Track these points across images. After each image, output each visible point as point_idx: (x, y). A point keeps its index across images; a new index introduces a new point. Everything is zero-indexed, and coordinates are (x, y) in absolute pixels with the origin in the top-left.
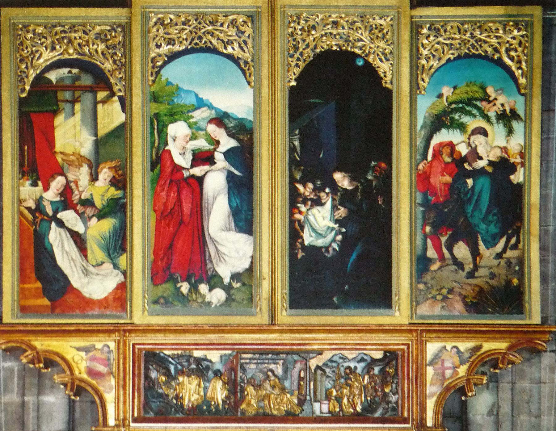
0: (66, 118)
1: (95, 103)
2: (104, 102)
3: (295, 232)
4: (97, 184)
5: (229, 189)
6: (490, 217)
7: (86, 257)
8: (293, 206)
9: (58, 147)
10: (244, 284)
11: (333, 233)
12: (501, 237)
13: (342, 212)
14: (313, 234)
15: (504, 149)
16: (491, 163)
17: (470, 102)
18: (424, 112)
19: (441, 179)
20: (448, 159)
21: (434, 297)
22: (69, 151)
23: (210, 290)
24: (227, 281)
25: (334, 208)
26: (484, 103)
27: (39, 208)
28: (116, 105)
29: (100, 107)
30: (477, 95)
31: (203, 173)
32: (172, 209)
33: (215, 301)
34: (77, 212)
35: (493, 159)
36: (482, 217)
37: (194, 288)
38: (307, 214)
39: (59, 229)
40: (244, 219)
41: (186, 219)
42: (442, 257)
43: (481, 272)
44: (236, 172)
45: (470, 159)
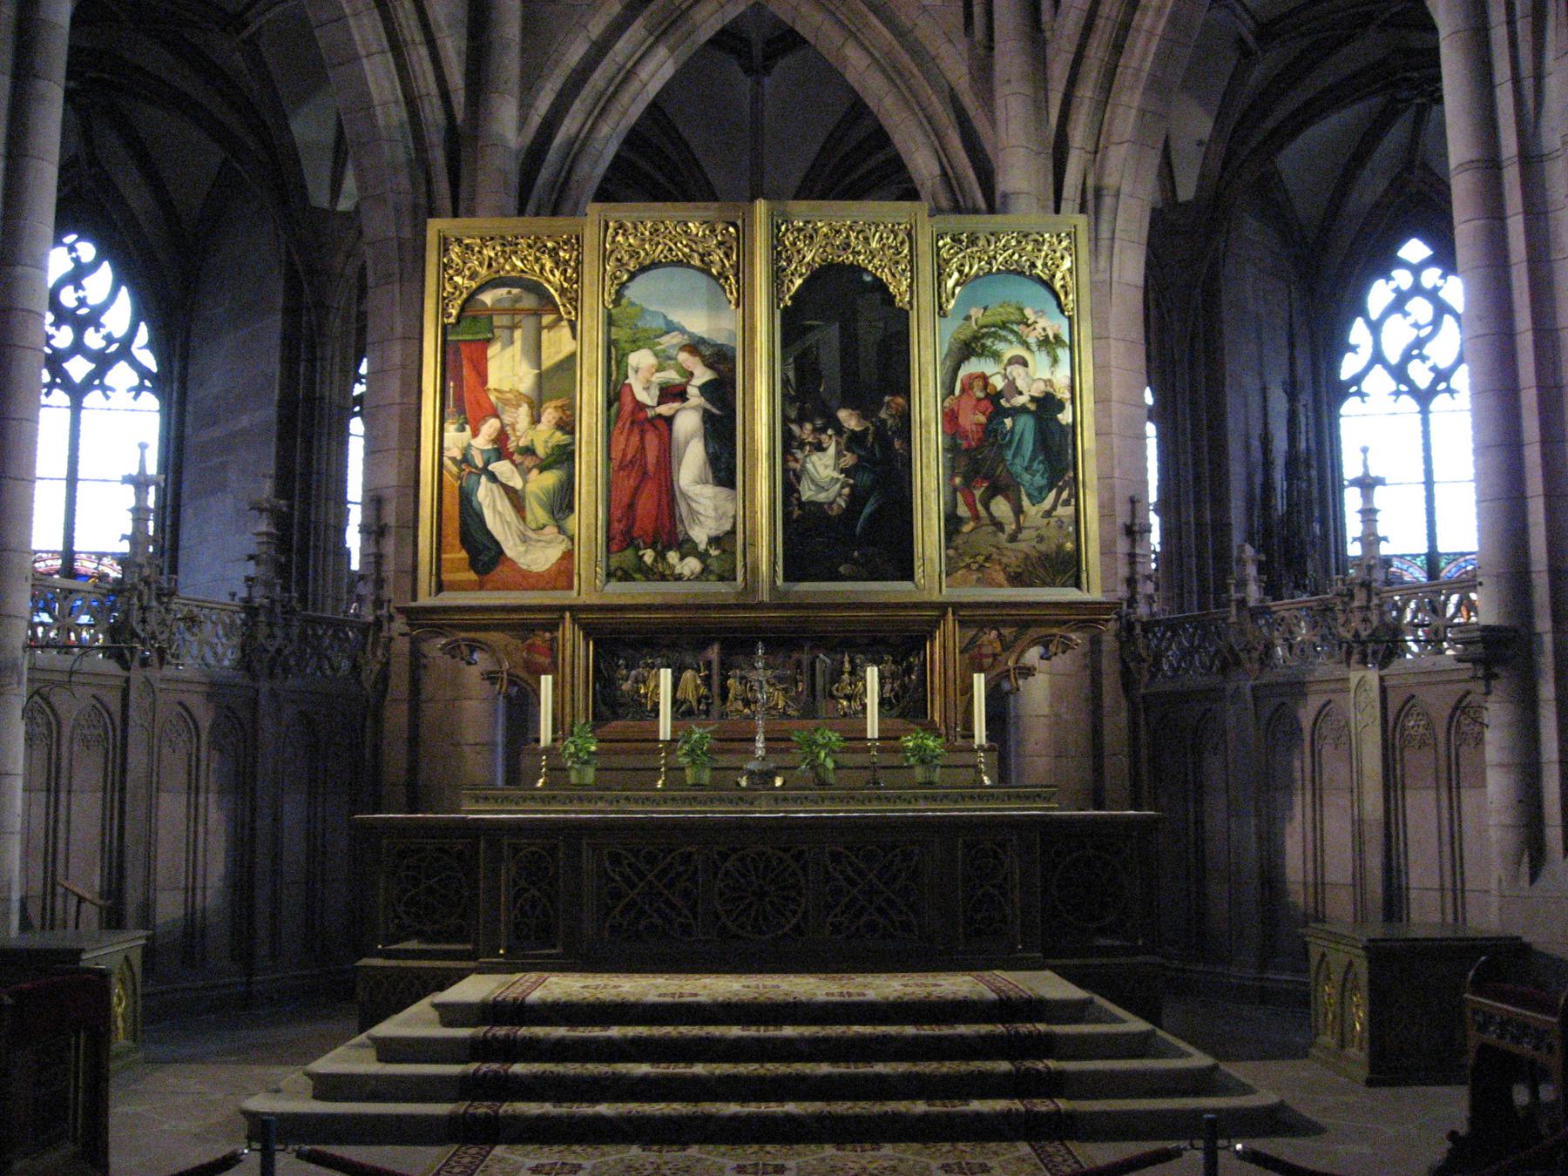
0: (503, 348)
1: (540, 329)
2: (550, 327)
3: (790, 483)
4: (540, 427)
6: (1035, 466)
7: (524, 519)
9: (492, 382)
10: (724, 551)
13: (849, 459)
15: (1048, 382)
16: (1033, 399)
17: (1004, 326)
18: (947, 339)
19: (973, 419)
20: (981, 395)
21: (968, 566)
22: (506, 388)
23: (682, 559)
24: (702, 547)
25: (839, 454)
26: (1022, 327)
27: (466, 459)
29: (545, 333)
33: (687, 572)
34: (513, 462)
37: (661, 556)
40: (723, 470)
41: (651, 468)
43: (1024, 535)
44: (715, 411)
45: (1006, 393)
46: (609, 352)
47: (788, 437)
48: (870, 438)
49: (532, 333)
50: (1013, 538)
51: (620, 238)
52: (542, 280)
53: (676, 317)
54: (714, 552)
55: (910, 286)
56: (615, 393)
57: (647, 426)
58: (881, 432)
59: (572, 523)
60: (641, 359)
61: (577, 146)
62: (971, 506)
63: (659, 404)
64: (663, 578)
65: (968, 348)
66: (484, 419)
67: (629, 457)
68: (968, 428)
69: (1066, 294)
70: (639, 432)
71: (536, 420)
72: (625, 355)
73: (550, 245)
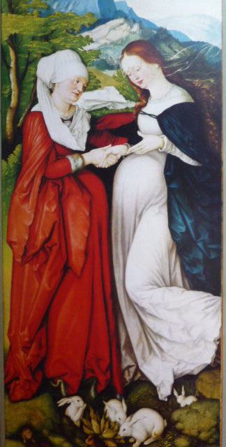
5: (171, 192)
10: (201, 398)
23: (130, 412)
24: (164, 392)
31: (112, 161)
32: (47, 240)
37: (95, 408)
41: (77, 260)
44: (186, 159)
54: (184, 400)
57: (70, 186)
63: (90, 146)
72: (32, 62)
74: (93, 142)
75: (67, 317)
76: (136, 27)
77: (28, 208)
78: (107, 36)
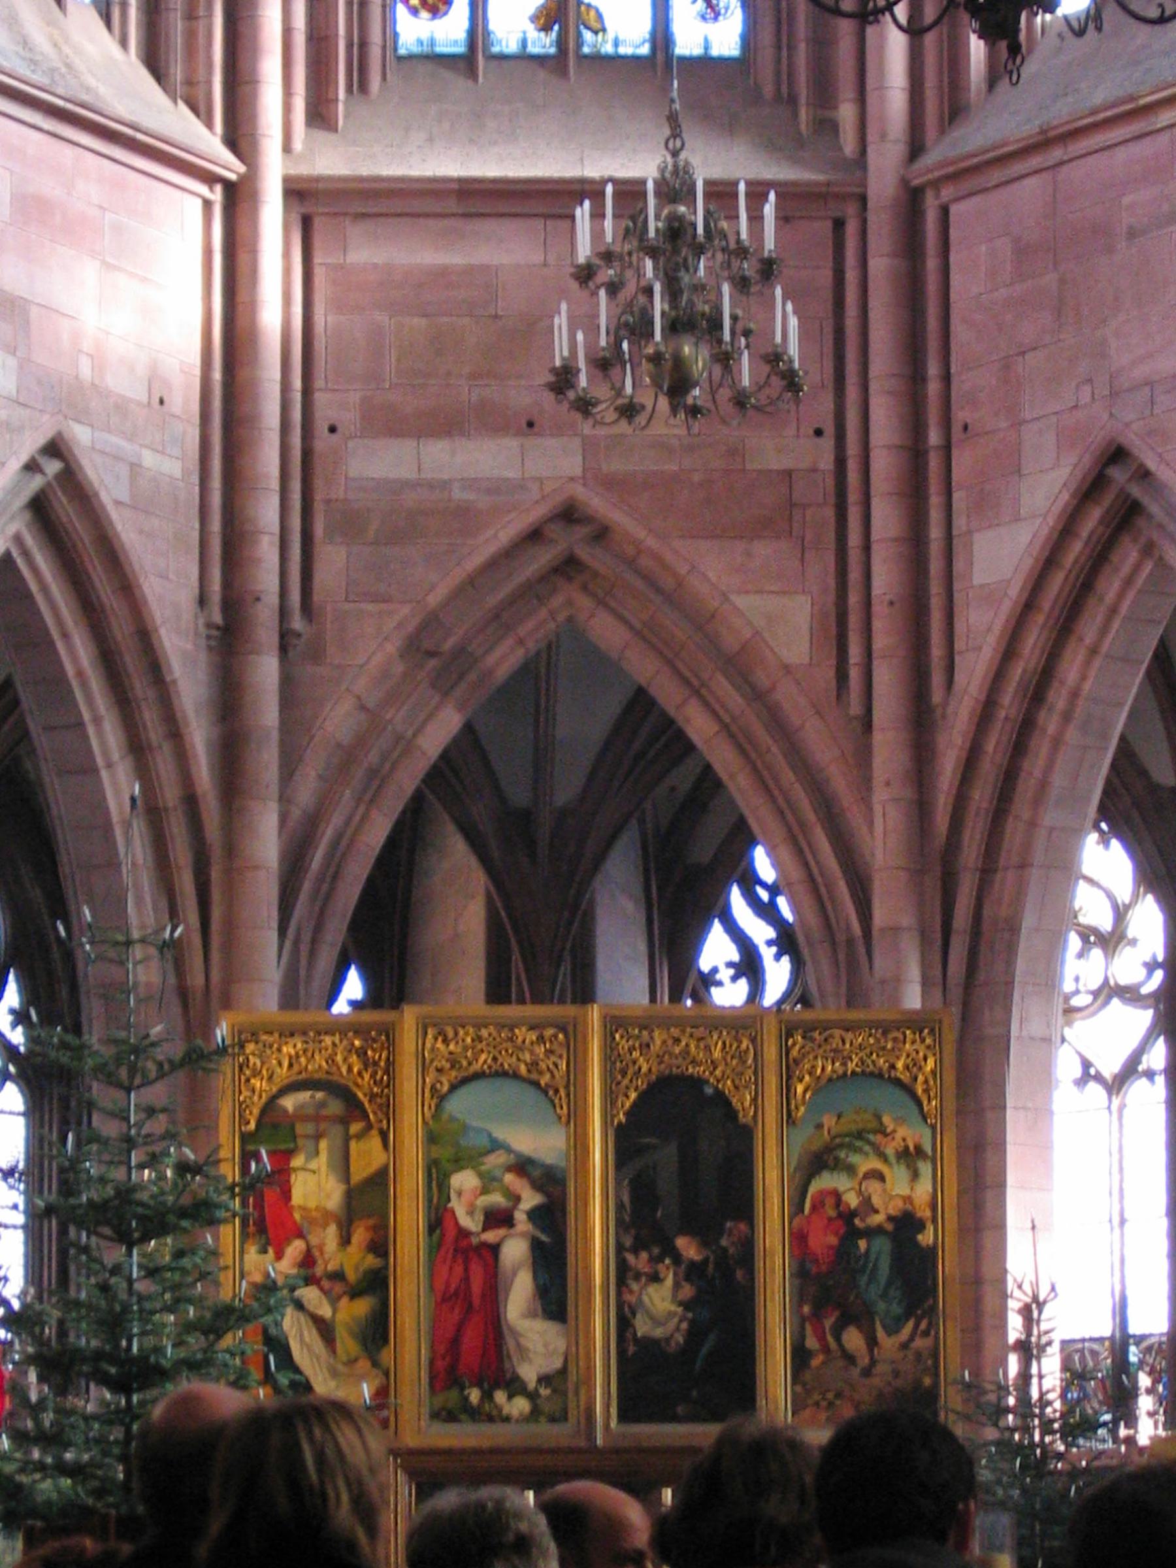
2: (359, 1136)
6: (892, 1292)
7: (334, 1352)
8: (621, 1282)
9: (297, 1198)
10: (554, 1391)
11: (676, 1320)
12: (907, 1320)
13: (687, 1291)
14: (649, 1322)
15: (908, 1199)
16: (890, 1218)
17: (859, 1135)
19: (824, 1240)
20: (832, 1213)
21: (817, 1404)
22: (312, 1204)
23: (510, 1397)
24: (532, 1385)
25: (677, 1286)
28: (375, 1142)
29: (353, 1145)
30: (869, 1126)
31: (497, 1240)
33: (515, 1413)
34: (321, 1289)
35: (892, 1212)
36: (880, 1293)
37: (488, 1396)
38: (641, 1294)
39: (296, 1313)
40: (554, 1301)
41: (476, 1301)
42: (826, 1349)
43: (880, 1368)
44: (544, 1238)
46: (430, 1175)
47: (623, 1270)
48: (711, 1266)
49: (339, 1142)
50: (867, 1372)
51: (439, 1045)
52: (351, 1084)
53: (501, 1133)
54: (544, 1392)
55: (754, 1100)
56: (439, 1219)
58: (723, 1262)
59: (386, 1356)
60: (464, 1180)
61: (344, 842)
62: (822, 1339)
63: (485, 1229)
64: (491, 1419)
65: (820, 1160)
66: (288, 1241)
67: (452, 1290)
68: (819, 1251)
69: (929, 1101)
70: (467, 1262)
71: (345, 1241)
72: (447, 1176)
73: (357, 1043)
74: (485, 1228)
75: (471, 1339)
76: (512, 1156)
77: (445, 1271)
78: (496, 1160)
